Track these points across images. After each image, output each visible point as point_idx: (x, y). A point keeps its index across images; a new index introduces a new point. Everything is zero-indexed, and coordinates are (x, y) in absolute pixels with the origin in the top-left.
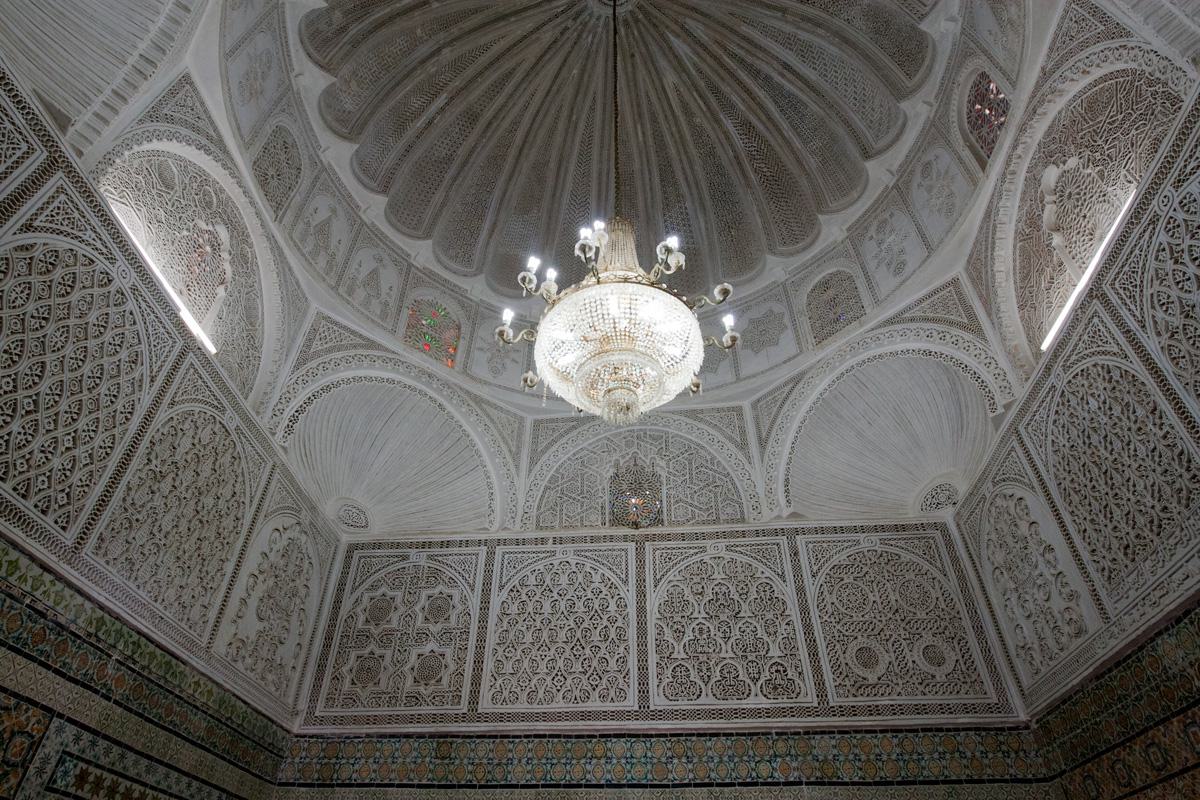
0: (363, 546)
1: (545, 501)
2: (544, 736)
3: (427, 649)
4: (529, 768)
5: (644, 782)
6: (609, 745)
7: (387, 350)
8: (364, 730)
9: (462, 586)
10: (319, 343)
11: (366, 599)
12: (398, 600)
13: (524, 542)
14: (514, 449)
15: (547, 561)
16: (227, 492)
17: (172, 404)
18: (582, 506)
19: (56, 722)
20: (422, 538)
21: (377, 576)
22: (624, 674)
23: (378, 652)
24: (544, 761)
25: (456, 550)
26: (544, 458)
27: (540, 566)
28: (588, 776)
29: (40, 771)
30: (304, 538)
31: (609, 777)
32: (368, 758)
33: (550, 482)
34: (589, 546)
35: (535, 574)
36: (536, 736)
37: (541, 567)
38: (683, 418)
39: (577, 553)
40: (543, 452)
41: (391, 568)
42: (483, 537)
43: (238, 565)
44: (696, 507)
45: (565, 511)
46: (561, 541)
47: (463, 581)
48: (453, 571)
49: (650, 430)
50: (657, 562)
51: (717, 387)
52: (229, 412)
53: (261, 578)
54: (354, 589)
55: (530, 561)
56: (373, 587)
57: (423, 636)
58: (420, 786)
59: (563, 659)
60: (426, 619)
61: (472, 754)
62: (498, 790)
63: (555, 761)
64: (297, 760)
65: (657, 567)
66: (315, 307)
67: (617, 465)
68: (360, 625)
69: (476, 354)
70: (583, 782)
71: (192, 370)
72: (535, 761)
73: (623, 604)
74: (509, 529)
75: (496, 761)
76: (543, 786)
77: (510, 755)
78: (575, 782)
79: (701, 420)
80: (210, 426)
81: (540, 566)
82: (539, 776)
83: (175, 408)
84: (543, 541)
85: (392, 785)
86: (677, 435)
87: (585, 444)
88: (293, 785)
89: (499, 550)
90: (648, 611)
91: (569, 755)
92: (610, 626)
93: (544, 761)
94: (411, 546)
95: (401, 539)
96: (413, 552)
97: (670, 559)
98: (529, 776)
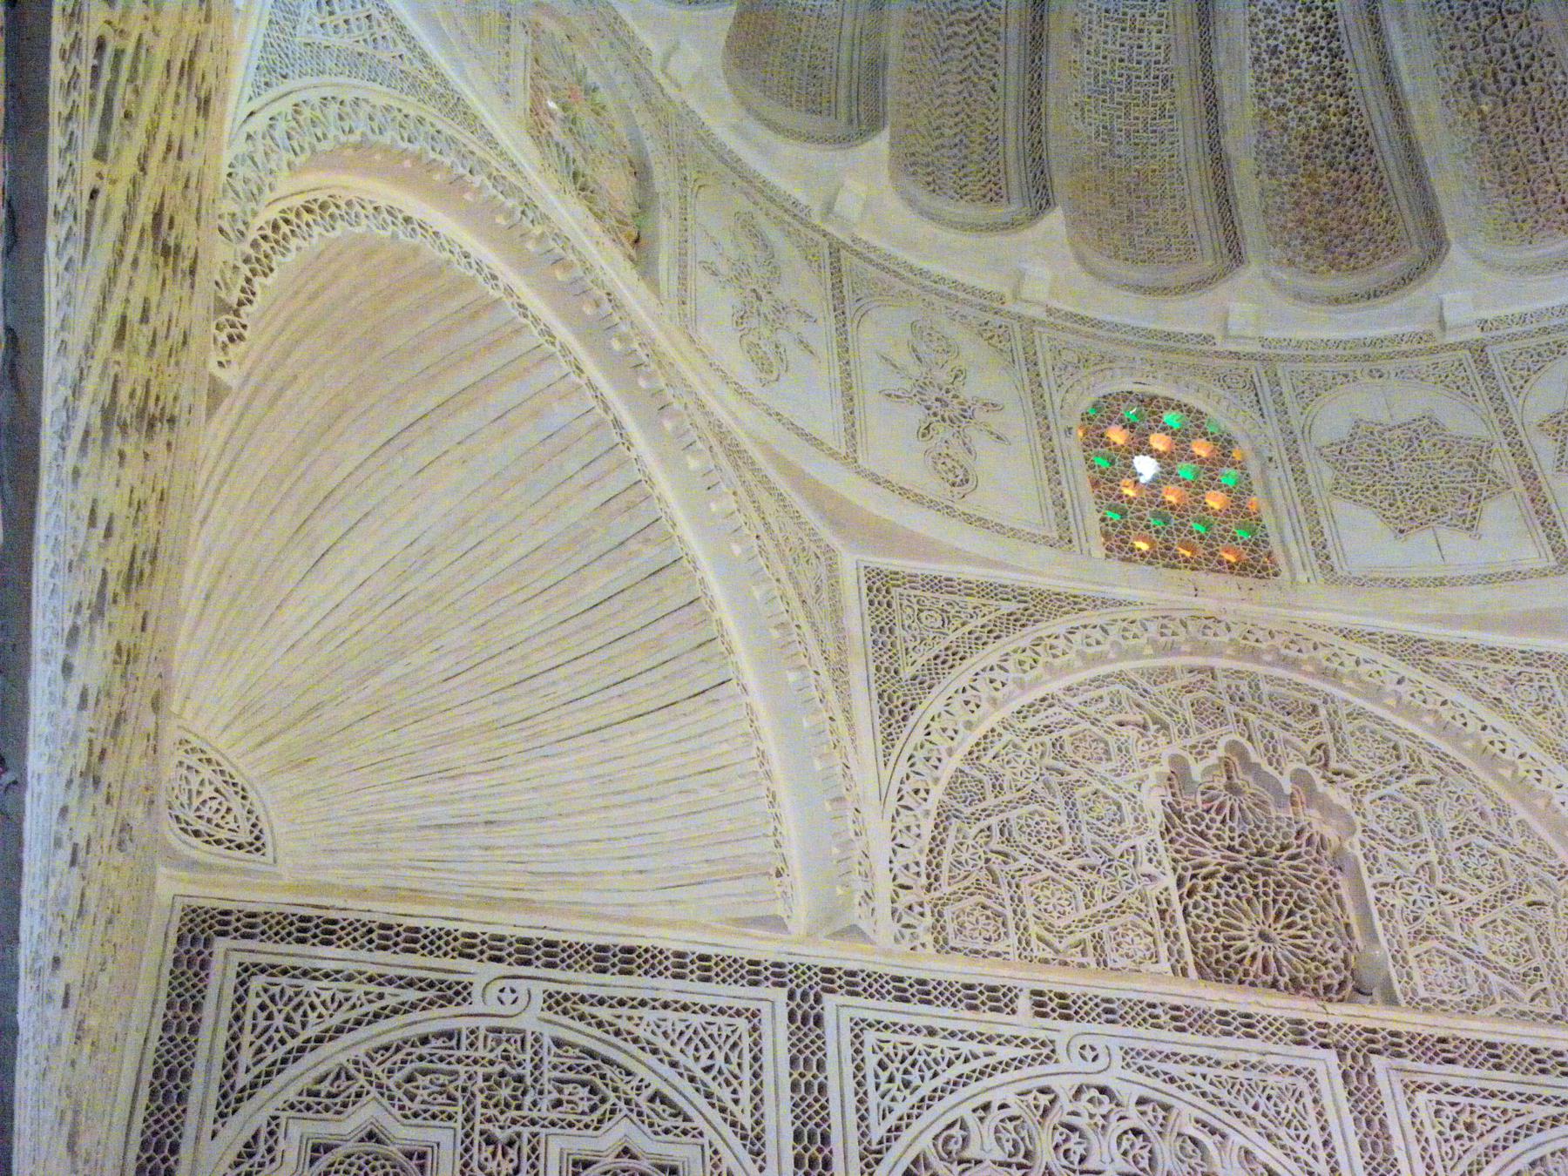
0: (250, 925)
1: (947, 859)
7: (491, 142)
9: (710, 1134)
11: (298, 1133)
13: (924, 992)
18: (1089, 895)
20: (511, 924)
21: (334, 1054)
25: (667, 988)
26: (932, 704)
27: (1003, 1089)
33: (950, 791)
34: (1167, 1039)
38: (1386, 659)
40: (923, 683)
41: (391, 1030)
42: (766, 948)
44: (1486, 962)
45: (1031, 910)
46: (1066, 1008)
47: (715, 1116)
48: (670, 1073)
49: (1270, 680)
50: (1430, 1133)
51: (1488, 579)
55: (960, 1068)
56: (313, 1101)
65: (1433, 1149)
67: (1178, 777)
69: (702, 282)
74: (862, 934)
79: (1445, 676)
81: (1003, 1089)
84: (998, 998)
86: (1361, 713)
87: (1055, 686)
94: (469, 946)
95: (426, 916)
96: (480, 972)
97: (1469, 1127)
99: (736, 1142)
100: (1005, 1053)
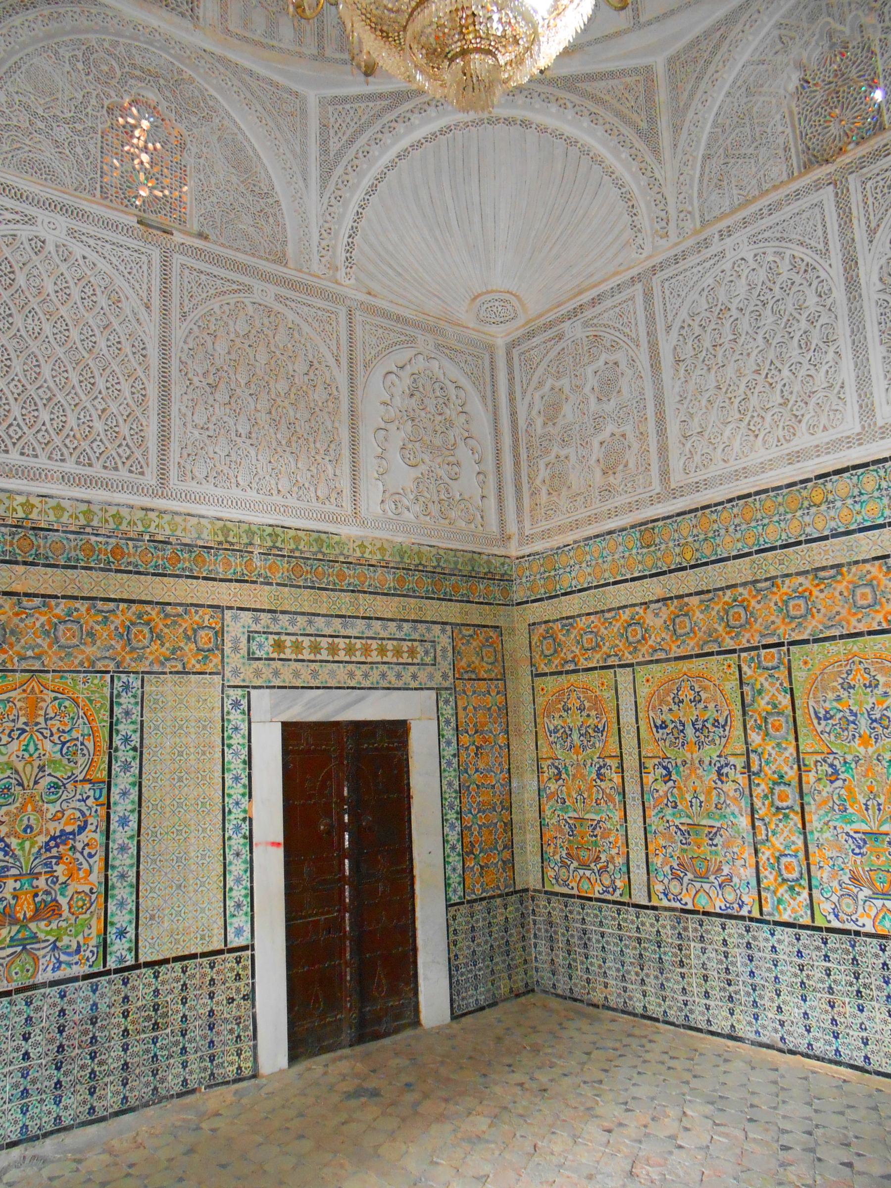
2: (749, 495)
3: (605, 435)
4: (738, 535)
5: (880, 521)
6: (829, 486)
8: (569, 538)
10: (336, 139)
11: (537, 396)
12: (567, 389)
13: (684, 255)
14: (644, 125)
15: (717, 269)
16: (301, 366)
17: (184, 315)
19: (228, 614)
22: (837, 388)
23: (563, 453)
24: (753, 524)
28: (808, 530)
29: (236, 649)
30: (435, 364)
31: (833, 524)
32: (581, 563)
33: (708, 146)
35: (705, 293)
36: (740, 498)
37: (710, 281)
39: (754, 240)
41: (552, 354)
43: (353, 428)
47: (625, 339)
48: (612, 331)
52: (258, 285)
53: (392, 427)
54: (524, 392)
55: (695, 279)
57: (599, 421)
58: (633, 579)
59: (756, 394)
60: (599, 400)
61: (676, 535)
62: (710, 567)
63: (766, 521)
64: (524, 580)
66: (312, 97)
68: (539, 431)
70: (803, 538)
71: (187, 272)
72: (744, 527)
73: (826, 288)
75: (702, 537)
76: (757, 552)
77: (715, 527)
78: (793, 540)
80: (242, 313)
82: (750, 541)
83: (189, 318)
85: (608, 584)
88: (527, 602)
89: (656, 280)
90: (863, 286)
91: (782, 509)
92: (811, 328)
93: (753, 524)
98: (739, 545)
99: (631, 344)
100: (707, 265)
